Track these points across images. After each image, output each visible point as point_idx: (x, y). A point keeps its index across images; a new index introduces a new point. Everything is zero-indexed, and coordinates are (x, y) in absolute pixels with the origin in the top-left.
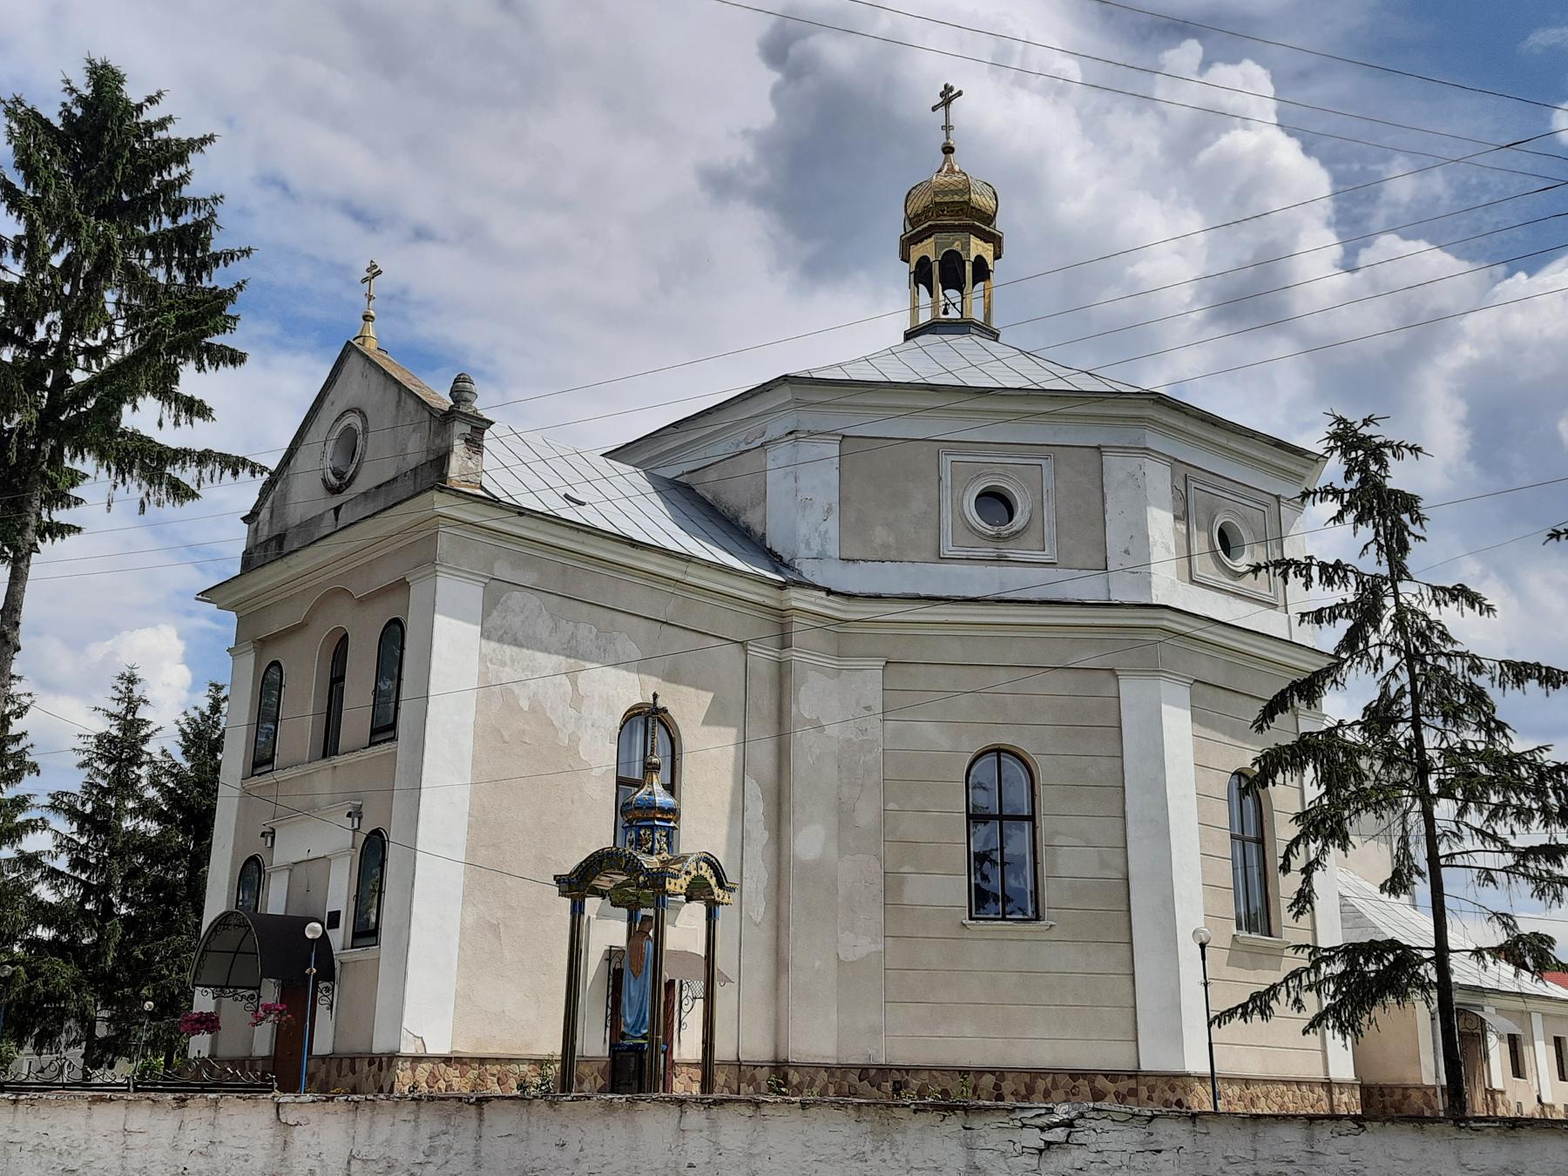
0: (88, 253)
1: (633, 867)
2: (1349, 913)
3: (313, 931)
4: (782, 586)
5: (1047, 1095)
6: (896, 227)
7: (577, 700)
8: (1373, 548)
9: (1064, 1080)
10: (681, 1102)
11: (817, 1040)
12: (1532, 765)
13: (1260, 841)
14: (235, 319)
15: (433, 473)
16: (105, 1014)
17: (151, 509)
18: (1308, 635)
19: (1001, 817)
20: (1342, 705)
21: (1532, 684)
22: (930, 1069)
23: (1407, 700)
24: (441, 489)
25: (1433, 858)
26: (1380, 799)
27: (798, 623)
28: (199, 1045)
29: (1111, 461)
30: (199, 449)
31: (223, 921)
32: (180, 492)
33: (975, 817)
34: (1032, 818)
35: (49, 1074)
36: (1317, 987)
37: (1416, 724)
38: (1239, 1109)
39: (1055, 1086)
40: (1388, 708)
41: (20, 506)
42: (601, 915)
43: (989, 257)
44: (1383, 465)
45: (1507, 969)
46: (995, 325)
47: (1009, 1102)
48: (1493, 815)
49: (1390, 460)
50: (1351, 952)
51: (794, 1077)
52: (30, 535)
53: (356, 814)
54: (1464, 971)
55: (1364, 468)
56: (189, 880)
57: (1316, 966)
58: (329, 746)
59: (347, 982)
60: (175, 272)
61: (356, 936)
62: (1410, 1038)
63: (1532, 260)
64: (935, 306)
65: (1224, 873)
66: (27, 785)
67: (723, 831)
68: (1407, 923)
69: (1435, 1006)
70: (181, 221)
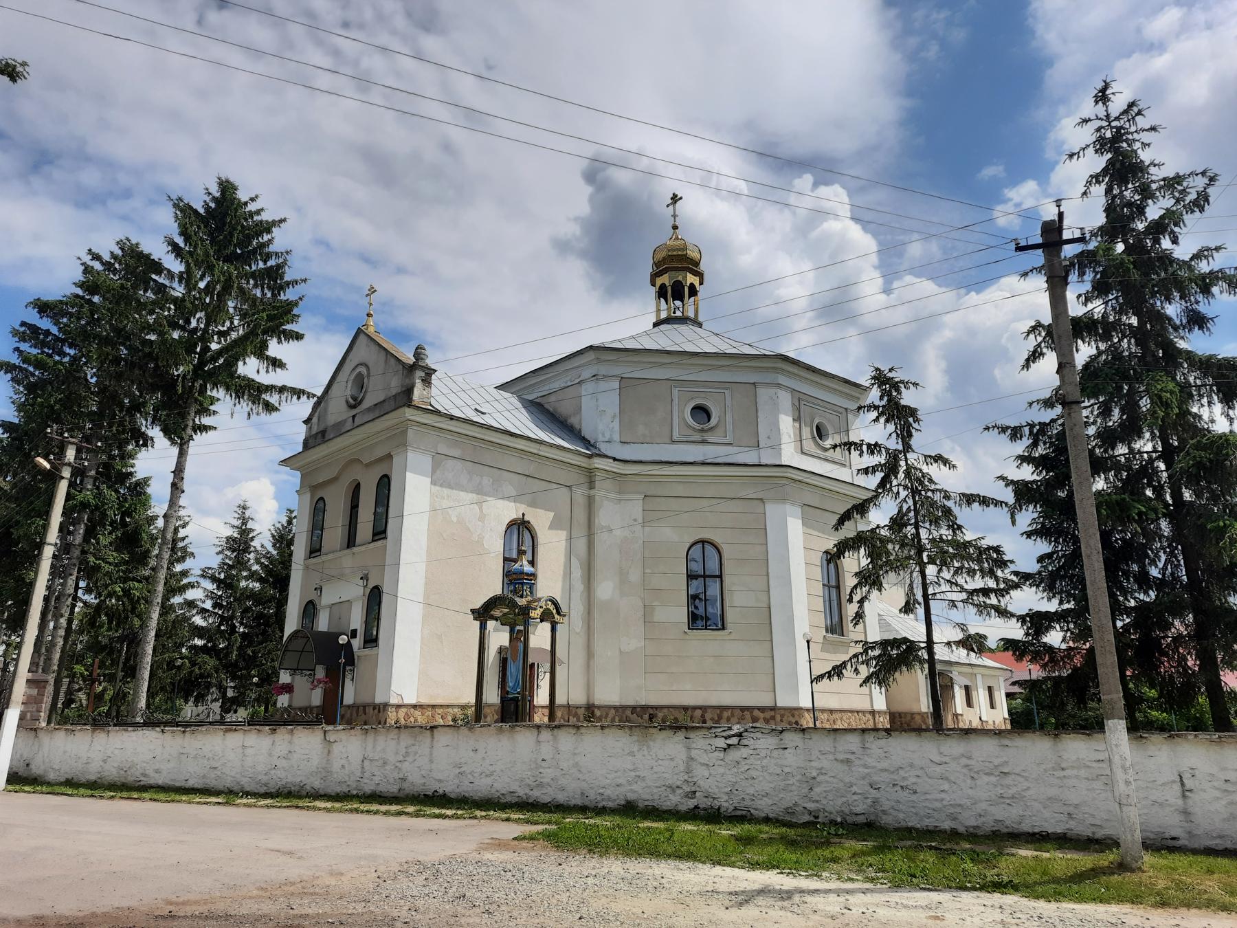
0: (219, 281)
1: (512, 604)
2: (883, 623)
3: (343, 639)
4: (590, 457)
5: (728, 720)
6: (649, 268)
7: (482, 518)
8: (894, 435)
9: (738, 712)
10: (538, 727)
11: (609, 693)
12: (975, 547)
13: (838, 587)
14: (298, 316)
15: (405, 397)
16: (232, 684)
17: (254, 417)
18: (861, 480)
19: (705, 576)
20: (879, 516)
21: (976, 505)
22: (668, 707)
23: (912, 514)
24: (409, 406)
25: (926, 596)
26: (897, 565)
27: (599, 476)
28: (283, 700)
29: (763, 393)
30: (280, 385)
31: (294, 635)
32: (269, 408)
33: (691, 577)
34: (720, 576)
35: (202, 717)
36: (867, 663)
37: (917, 527)
38: (828, 726)
39: (733, 715)
40: (902, 518)
41: (183, 416)
42: (496, 630)
43: (697, 284)
44: (899, 392)
45: (963, 652)
46: (700, 319)
47: (709, 724)
48: (956, 573)
49: (903, 389)
50: (884, 644)
51: (598, 713)
52: (189, 431)
53: (365, 578)
54: (941, 653)
55: (890, 395)
56: (276, 614)
57: (866, 651)
58: (351, 542)
59: (361, 668)
60: (266, 291)
61: (365, 642)
62: (913, 689)
63: (980, 285)
64: (669, 309)
65: (819, 604)
66: (188, 564)
67: (559, 584)
68: (912, 628)
69: (927, 671)
70: (269, 264)
